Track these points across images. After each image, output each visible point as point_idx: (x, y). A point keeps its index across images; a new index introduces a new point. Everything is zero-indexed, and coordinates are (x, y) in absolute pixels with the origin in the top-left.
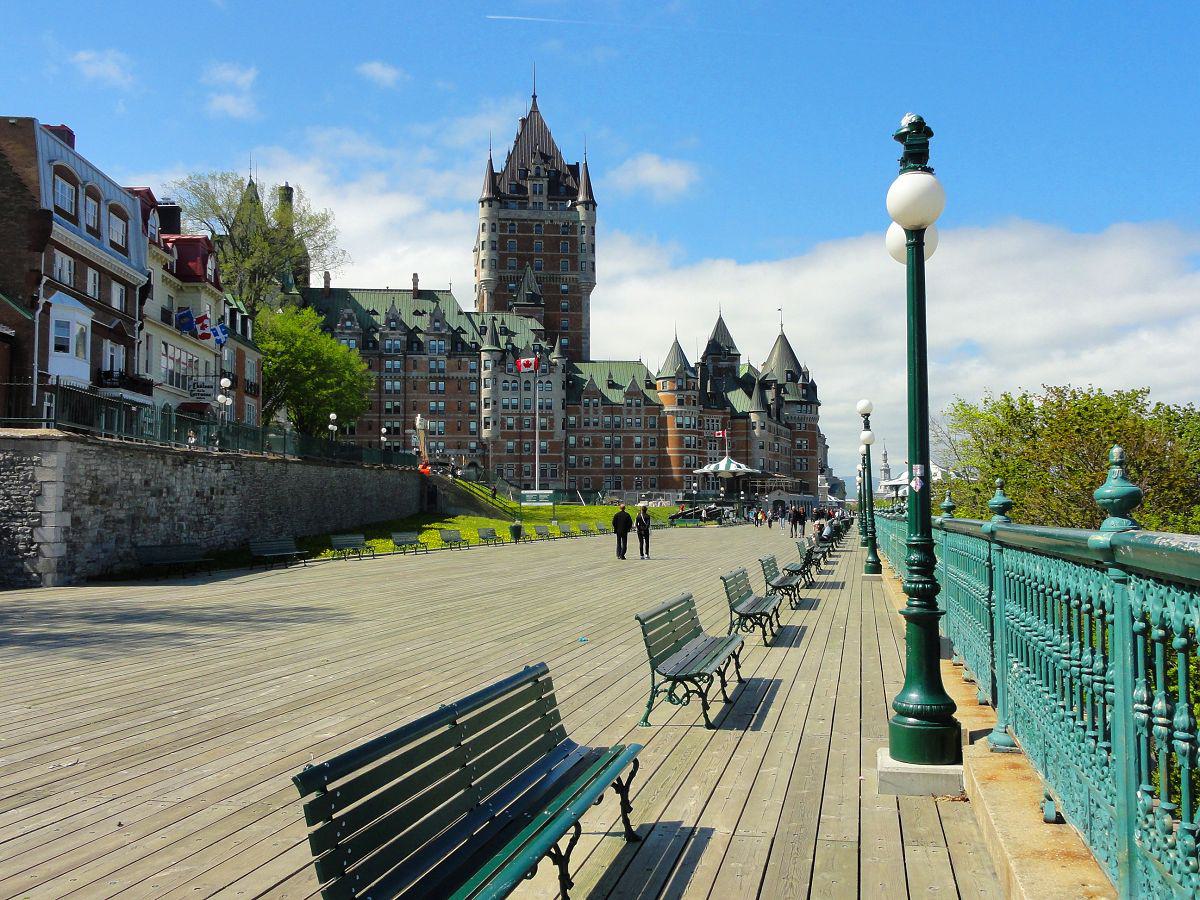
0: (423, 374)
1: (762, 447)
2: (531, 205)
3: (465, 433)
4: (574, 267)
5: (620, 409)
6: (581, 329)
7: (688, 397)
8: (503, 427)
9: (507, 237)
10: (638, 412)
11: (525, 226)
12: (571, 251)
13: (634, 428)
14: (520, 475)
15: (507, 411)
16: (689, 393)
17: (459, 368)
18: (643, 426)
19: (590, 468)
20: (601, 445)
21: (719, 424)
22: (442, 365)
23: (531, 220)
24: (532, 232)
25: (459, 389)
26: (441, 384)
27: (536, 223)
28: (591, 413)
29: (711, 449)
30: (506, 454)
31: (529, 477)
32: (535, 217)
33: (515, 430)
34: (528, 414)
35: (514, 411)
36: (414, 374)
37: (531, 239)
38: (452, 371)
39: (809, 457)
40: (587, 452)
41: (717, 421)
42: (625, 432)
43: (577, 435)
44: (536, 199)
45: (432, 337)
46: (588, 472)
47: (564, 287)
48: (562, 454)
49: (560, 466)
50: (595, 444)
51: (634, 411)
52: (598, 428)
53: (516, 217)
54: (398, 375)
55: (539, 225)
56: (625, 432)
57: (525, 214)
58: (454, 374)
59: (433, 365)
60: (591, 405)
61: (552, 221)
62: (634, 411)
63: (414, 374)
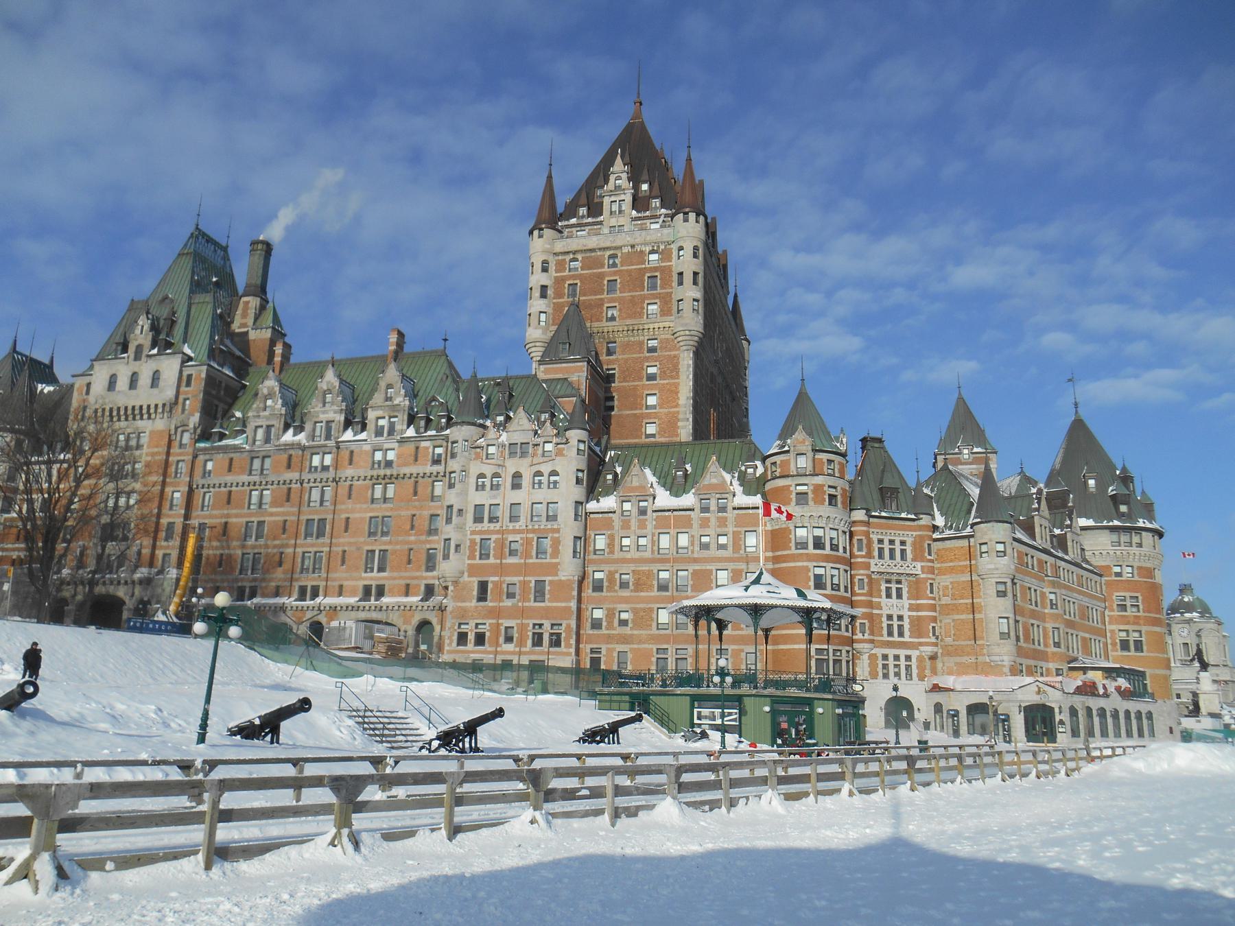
0: (362, 473)
1: (1001, 594)
2: (606, 230)
3: (418, 569)
4: (665, 311)
5: (689, 518)
6: (677, 406)
7: (818, 489)
8: (472, 557)
9: (563, 279)
10: (722, 522)
11: (591, 257)
12: (662, 287)
13: (713, 552)
14: (498, 645)
15: (479, 527)
16: (819, 480)
17: (416, 460)
18: (730, 548)
19: (627, 630)
20: (650, 587)
21: (909, 549)
22: (391, 456)
23: (600, 249)
24: (602, 266)
25: (415, 493)
26: (391, 488)
27: (608, 253)
28: (633, 528)
29: (889, 596)
30: (474, 603)
31: (510, 647)
32: (608, 244)
33: (492, 560)
34: (515, 532)
35: (492, 526)
36: (349, 472)
37: (601, 276)
38: (405, 465)
39: (1144, 629)
40: (626, 600)
41: (903, 543)
42: (695, 561)
43: (607, 568)
44: (613, 222)
45: (380, 413)
46: (625, 640)
47: (652, 343)
48: (573, 604)
49: (568, 626)
50: (639, 586)
51: (713, 522)
52: (648, 554)
53: (580, 248)
54: (325, 475)
55: (613, 256)
56: (695, 561)
57: (593, 242)
58: (407, 470)
59: (378, 456)
60: (635, 512)
61: (633, 246)
62: (713, 522)
63: (349, 472)
